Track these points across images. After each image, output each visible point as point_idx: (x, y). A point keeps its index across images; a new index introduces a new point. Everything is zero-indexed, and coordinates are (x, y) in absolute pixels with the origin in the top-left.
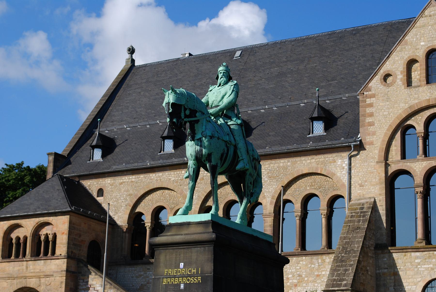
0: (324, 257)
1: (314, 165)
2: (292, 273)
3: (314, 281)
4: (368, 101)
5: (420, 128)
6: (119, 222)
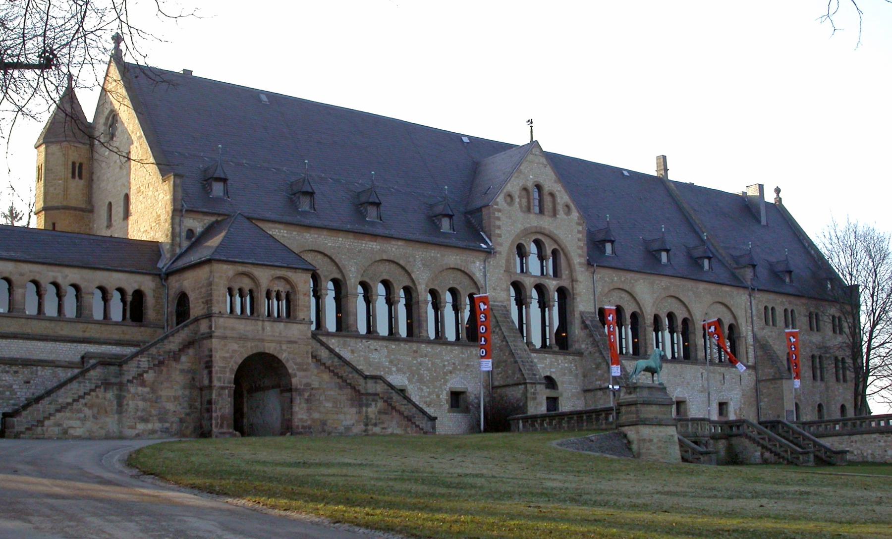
0: (472, 349)
1: (459, 261)
2: (448, 361)
3: (465, 370)
4: (497, 214)
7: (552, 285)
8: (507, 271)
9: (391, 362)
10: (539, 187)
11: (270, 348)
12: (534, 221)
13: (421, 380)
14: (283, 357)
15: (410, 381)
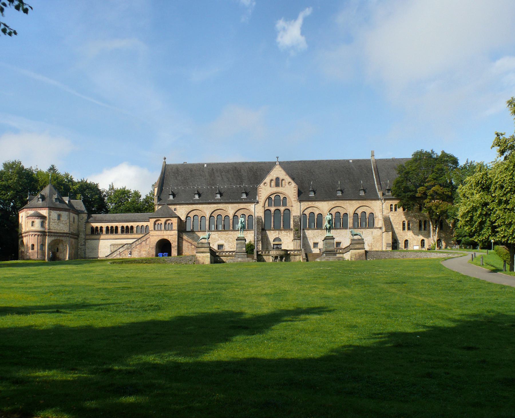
5: (273, 198)
6: (182, 219)
7: (282, 209)
8: (264, 206)
9: (219, 237)
10: (277, 179)
11: (166, 237)
12: (275, 189)
13: (229, 242)
14: (169, 239)
15: (225, 242)
